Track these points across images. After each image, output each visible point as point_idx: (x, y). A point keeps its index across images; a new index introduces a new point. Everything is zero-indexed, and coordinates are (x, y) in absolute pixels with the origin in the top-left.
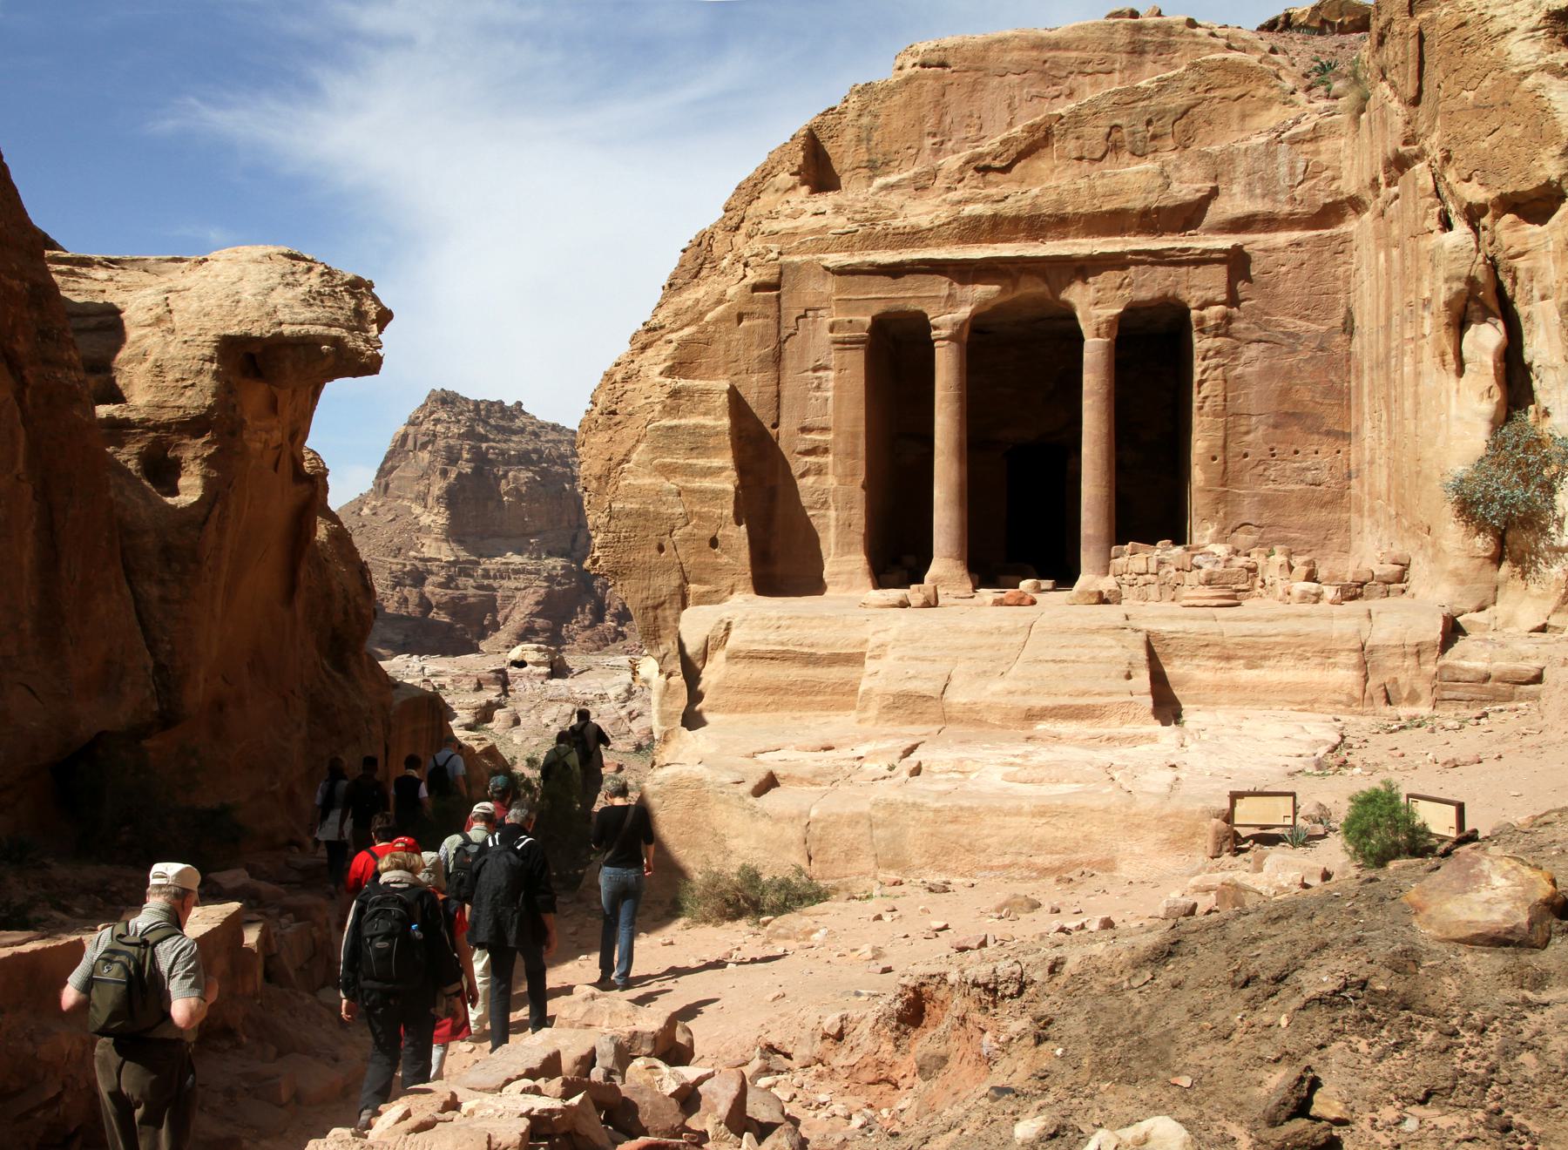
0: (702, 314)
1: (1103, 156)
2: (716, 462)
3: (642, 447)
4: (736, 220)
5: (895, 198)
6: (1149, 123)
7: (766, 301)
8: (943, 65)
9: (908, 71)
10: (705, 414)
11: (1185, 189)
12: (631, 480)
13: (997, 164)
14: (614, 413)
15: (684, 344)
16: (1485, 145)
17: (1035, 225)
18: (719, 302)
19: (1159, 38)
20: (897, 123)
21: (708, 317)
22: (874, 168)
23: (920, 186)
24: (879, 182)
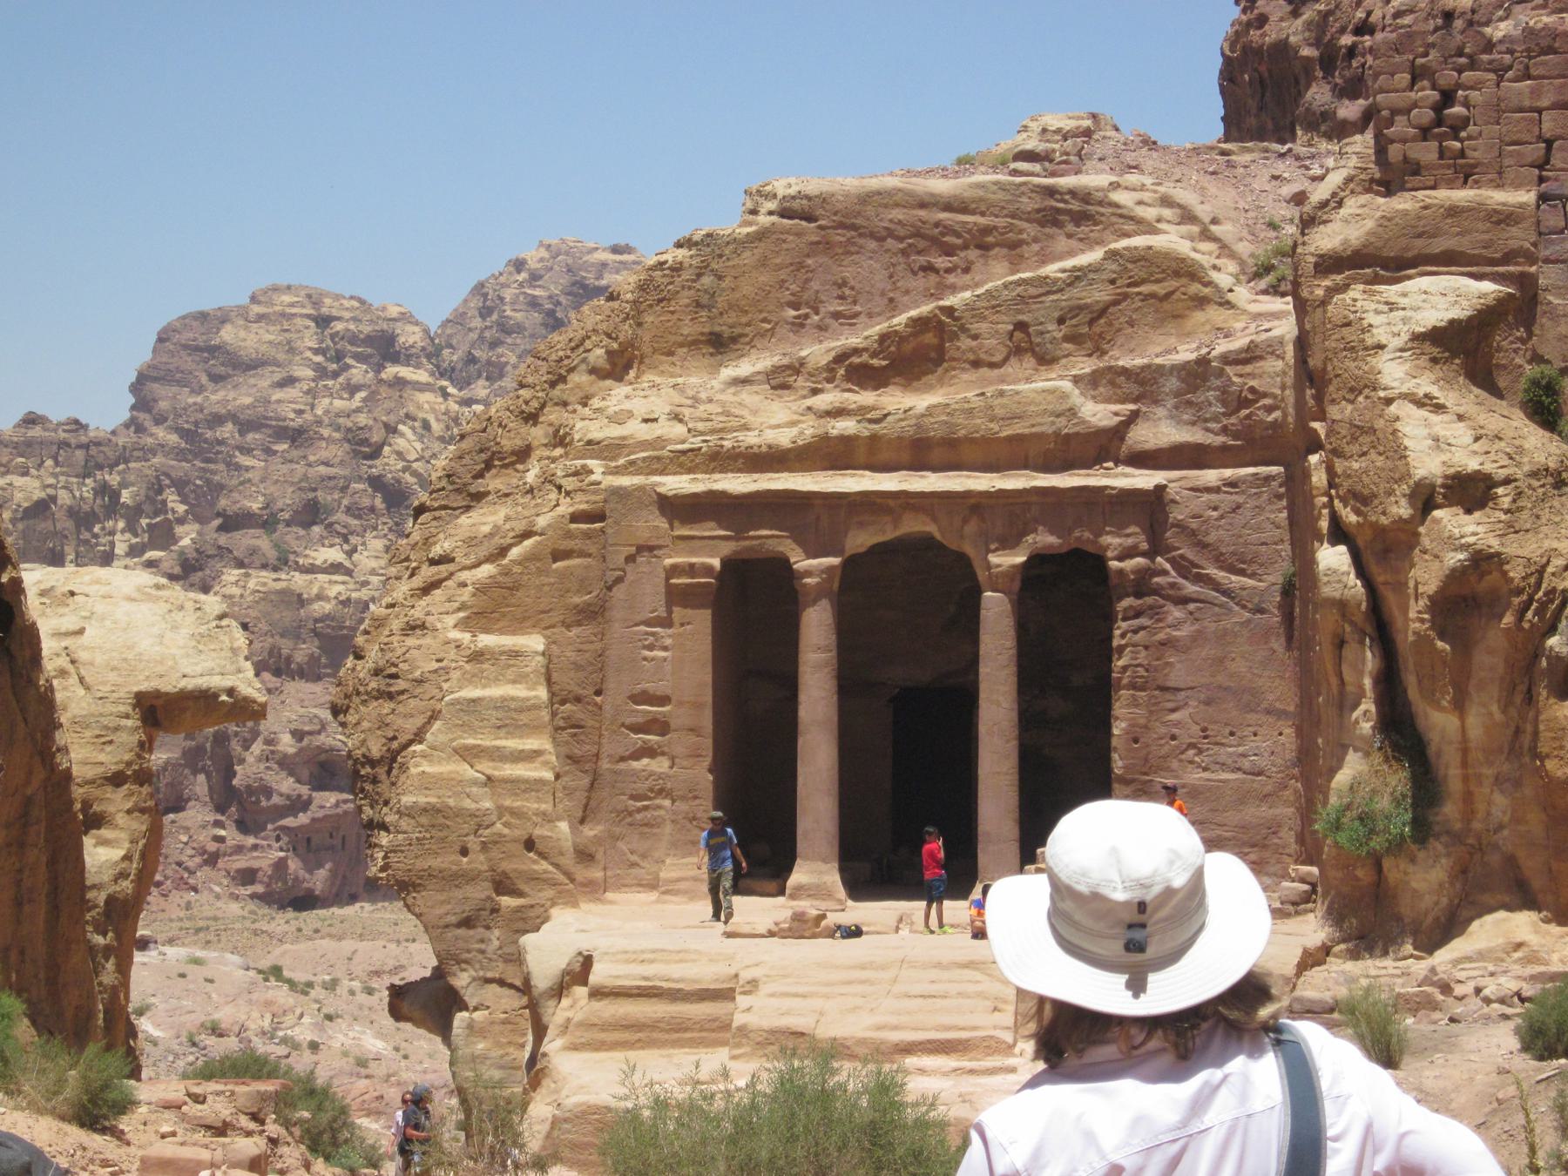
0: (503, 551)
1: (1006, 360)
2: (531, 744)
3: (437, 725)
4: (535, 404)
5: (748, 396)
6: (1061, 321)
7: (587, 535)
8: (810, 218)
9: (764, 220)
10: (514, 682)
11: (1098, 413)
12: (426, 767)
13: (875, 362)
14: (395, 676)
15: (482, 589)
16: (1356, 465)
17: (921, 451)
18: (527, 535)
19: (1075, 206)
20: (747, 289)
21: (515, 552)
22: (720, 345)
23: (780, 380)
24: (728, 372)
